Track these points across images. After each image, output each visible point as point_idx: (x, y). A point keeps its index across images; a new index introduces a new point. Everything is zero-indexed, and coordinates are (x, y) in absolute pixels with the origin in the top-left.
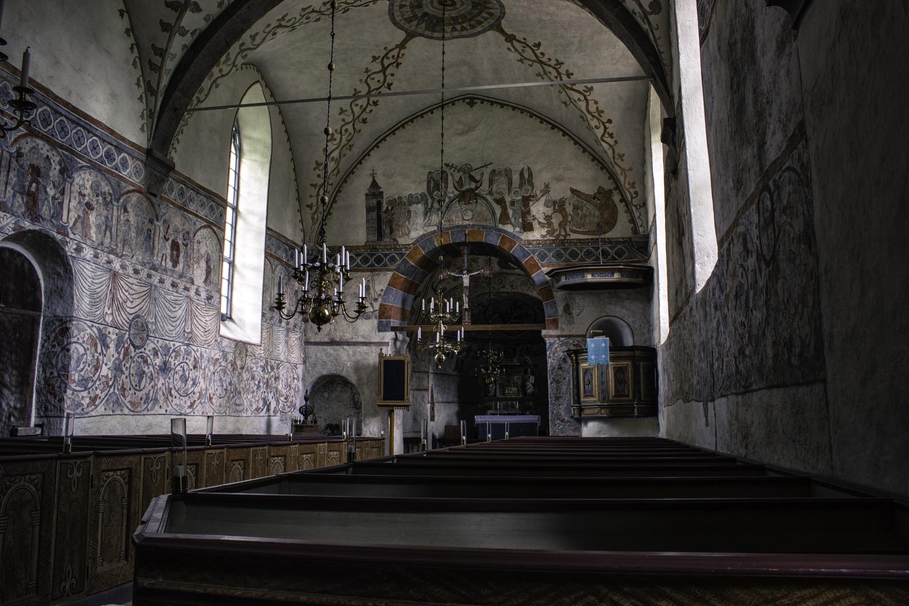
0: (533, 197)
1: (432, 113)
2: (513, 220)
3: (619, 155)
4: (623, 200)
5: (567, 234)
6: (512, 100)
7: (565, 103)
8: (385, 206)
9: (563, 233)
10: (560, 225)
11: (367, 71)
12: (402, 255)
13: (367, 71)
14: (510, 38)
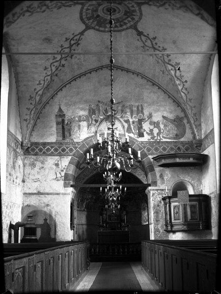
0: (144, 119)
1: (91, 73)
2: (133, 131)
3: (189, 99)
4: (189, 122)
5: (161, 139)
8: (66, 122)
9: (159, 138)
10: (157, 134)
12: (76, 148)
13: (62, 46)
14: (140, 34)
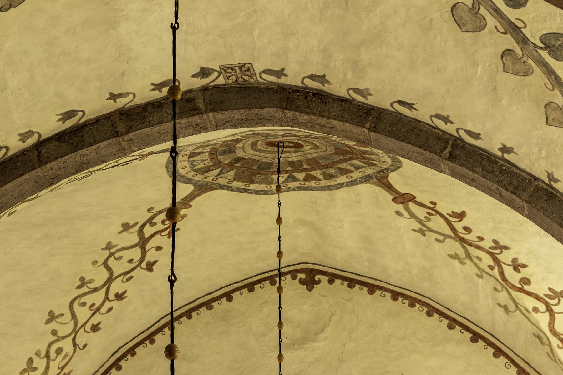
1: (230, 299)
6: (391, 281)
7: (506, 308)
11: (109, 246)
